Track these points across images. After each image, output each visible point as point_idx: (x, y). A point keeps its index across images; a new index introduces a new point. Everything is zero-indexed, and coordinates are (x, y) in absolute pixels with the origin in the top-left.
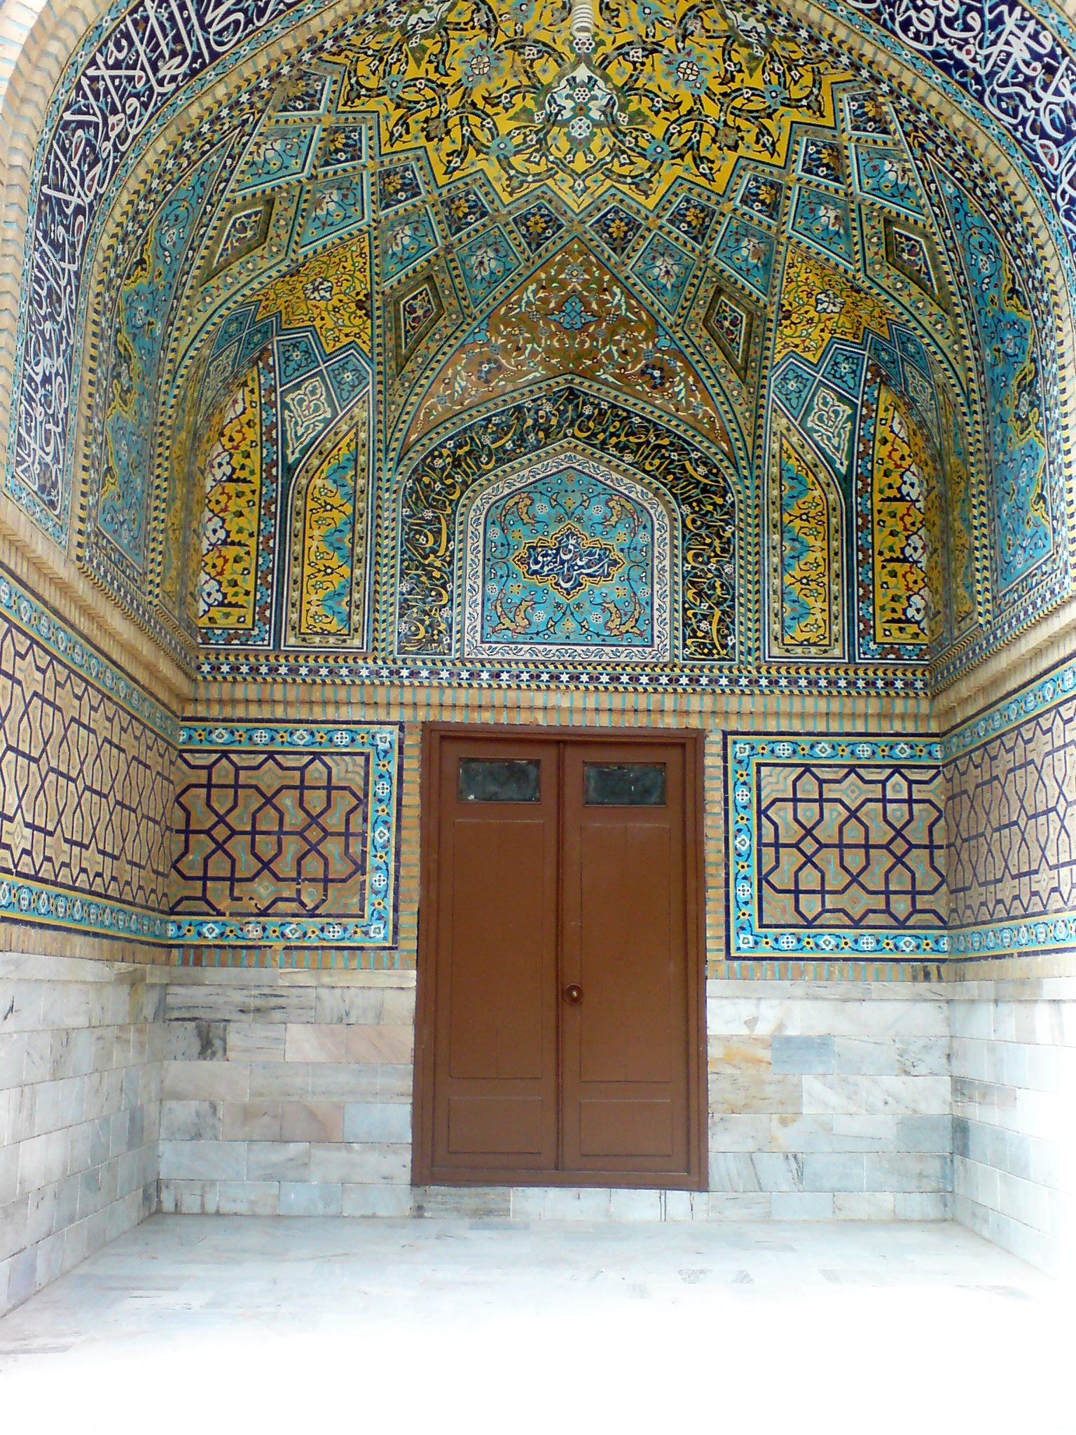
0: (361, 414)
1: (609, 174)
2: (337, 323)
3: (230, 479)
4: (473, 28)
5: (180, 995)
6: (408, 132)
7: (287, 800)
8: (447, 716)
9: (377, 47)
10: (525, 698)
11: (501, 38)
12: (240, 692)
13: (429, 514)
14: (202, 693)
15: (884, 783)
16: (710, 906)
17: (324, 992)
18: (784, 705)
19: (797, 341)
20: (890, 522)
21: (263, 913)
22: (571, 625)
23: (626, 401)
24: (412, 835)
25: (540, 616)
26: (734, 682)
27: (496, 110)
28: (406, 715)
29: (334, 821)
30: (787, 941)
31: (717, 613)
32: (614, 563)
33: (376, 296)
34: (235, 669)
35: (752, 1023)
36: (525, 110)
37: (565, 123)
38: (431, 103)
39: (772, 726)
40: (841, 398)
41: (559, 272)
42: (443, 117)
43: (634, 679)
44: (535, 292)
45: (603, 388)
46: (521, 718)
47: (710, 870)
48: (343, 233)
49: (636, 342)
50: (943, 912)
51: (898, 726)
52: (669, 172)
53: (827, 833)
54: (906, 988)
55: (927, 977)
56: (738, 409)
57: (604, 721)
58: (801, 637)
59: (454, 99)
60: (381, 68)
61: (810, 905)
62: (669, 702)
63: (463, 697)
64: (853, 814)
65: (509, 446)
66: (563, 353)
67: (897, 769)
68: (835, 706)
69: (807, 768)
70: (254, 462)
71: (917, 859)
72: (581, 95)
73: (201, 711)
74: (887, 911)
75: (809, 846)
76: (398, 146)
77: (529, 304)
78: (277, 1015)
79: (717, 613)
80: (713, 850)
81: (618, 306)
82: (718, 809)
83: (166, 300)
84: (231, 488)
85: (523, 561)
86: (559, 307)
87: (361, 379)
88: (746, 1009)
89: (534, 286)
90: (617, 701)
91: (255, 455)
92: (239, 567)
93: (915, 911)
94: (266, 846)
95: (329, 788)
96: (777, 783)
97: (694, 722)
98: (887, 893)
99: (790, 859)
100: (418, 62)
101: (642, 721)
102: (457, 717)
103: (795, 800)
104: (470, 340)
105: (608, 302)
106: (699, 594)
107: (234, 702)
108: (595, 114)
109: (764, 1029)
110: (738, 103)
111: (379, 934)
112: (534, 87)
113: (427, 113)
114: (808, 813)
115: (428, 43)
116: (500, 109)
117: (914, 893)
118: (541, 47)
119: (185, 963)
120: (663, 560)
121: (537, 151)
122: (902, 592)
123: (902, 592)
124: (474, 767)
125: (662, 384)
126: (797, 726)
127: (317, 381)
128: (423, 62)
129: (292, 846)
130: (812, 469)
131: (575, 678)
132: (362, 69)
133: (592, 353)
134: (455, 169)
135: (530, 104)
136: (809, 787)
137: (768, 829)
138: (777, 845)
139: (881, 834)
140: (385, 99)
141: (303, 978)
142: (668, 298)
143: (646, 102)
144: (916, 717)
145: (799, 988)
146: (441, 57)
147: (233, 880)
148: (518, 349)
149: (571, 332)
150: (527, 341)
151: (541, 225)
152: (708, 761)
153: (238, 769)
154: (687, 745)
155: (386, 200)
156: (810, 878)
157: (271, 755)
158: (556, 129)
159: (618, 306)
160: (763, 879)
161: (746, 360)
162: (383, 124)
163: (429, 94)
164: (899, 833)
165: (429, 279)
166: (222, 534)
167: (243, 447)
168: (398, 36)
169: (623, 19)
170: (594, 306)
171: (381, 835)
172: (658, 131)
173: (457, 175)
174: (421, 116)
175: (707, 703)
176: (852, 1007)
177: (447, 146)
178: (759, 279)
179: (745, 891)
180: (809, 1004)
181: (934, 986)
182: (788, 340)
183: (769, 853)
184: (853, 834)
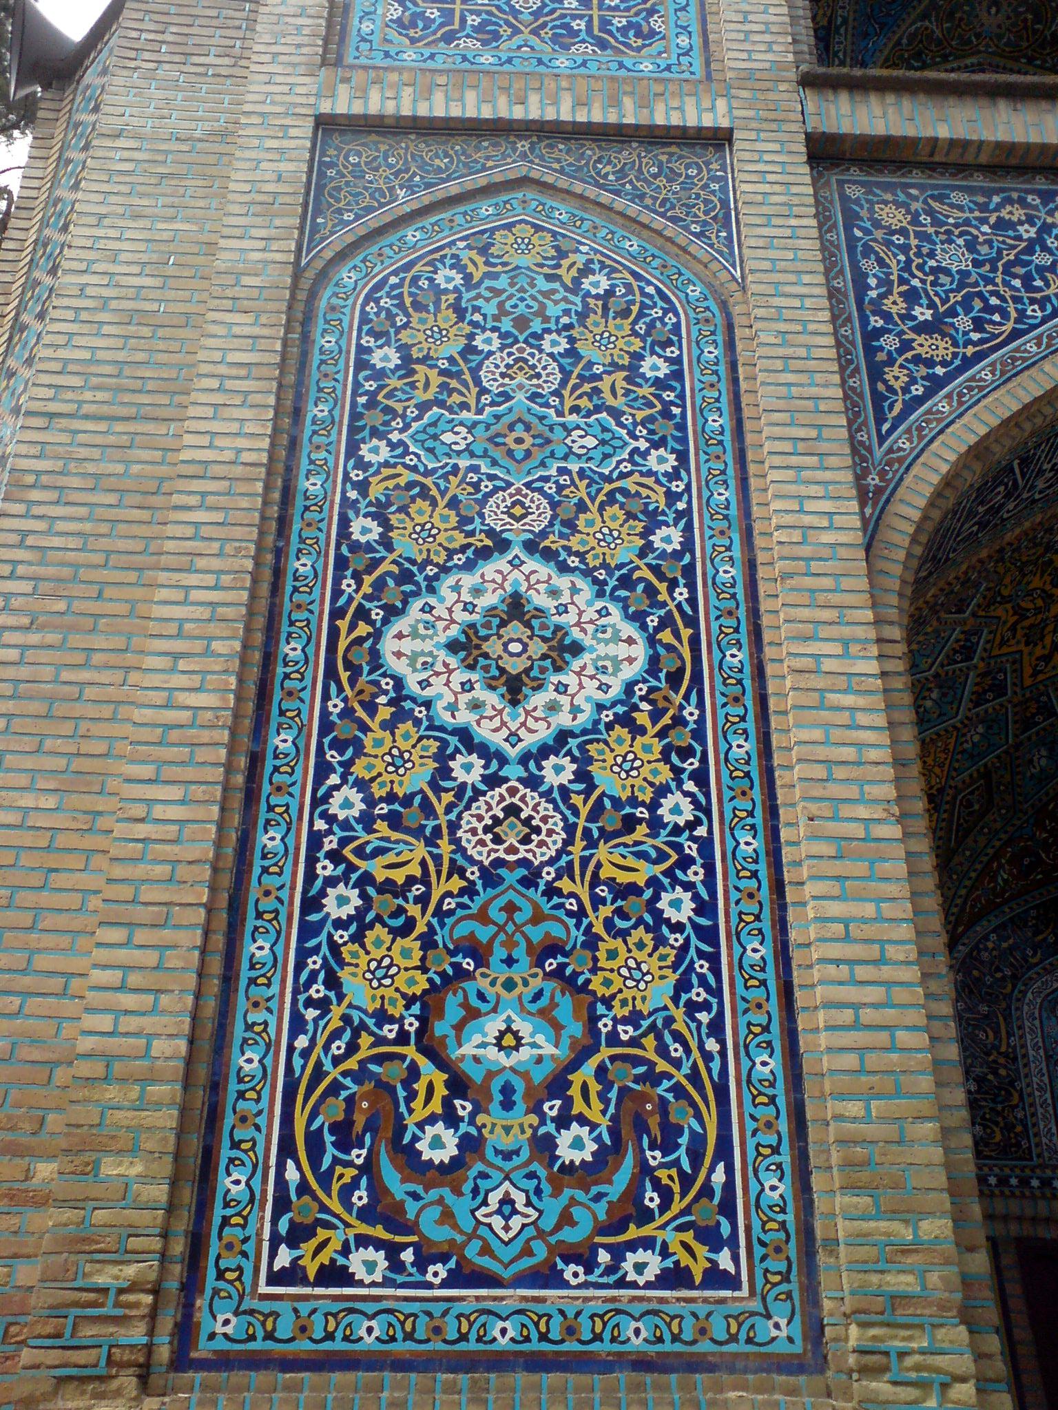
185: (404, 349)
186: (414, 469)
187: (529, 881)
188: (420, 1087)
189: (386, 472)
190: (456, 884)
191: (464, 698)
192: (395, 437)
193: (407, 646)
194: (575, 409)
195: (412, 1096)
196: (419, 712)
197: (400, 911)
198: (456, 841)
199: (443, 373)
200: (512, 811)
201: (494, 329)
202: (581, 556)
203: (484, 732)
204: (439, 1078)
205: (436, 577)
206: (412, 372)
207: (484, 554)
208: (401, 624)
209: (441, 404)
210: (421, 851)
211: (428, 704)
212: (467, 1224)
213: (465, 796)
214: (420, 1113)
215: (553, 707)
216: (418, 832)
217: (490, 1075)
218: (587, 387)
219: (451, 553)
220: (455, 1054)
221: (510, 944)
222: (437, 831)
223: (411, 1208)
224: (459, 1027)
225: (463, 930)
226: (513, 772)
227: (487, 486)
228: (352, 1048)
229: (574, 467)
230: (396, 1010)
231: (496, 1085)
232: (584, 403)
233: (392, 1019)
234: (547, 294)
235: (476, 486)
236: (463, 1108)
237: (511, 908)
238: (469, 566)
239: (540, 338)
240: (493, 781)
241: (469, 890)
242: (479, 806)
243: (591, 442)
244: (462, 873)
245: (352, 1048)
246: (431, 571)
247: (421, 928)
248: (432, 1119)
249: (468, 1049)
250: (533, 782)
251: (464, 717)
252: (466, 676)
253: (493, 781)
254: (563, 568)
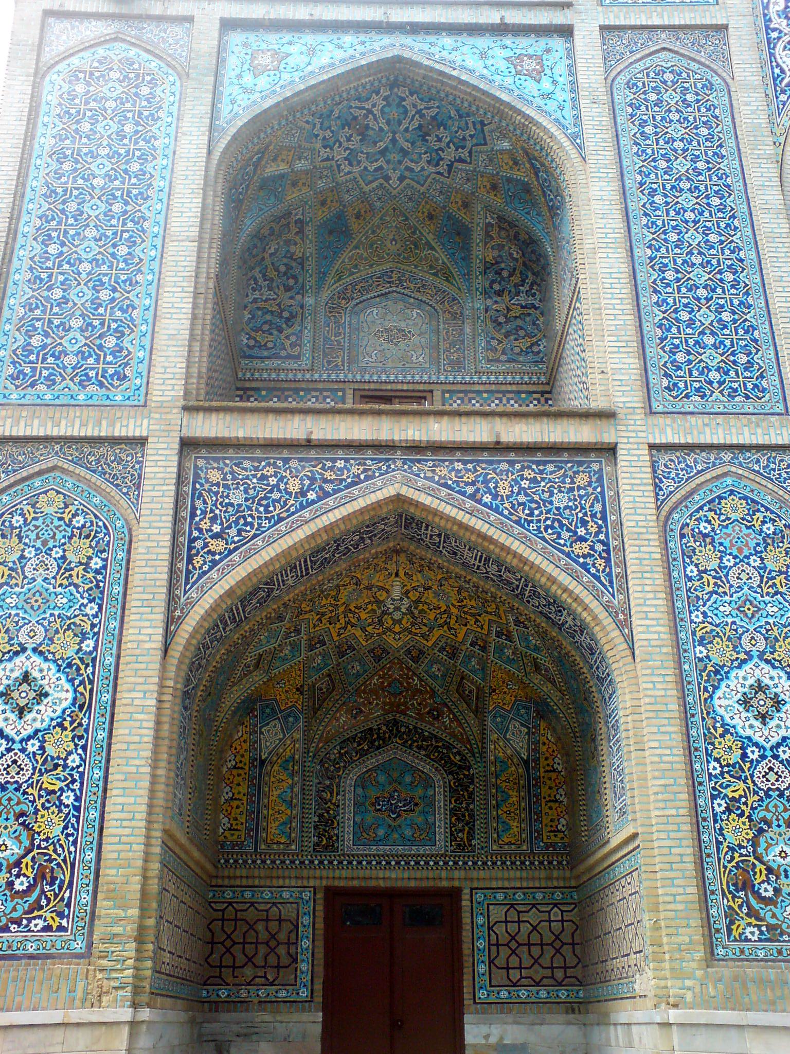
0: (296, 736)
2: (286, 696)
3: (235, 767)
5: (209, 1027)
7: (260, 927)
8: (336, 883)
10: (374, 873)
12: (238, 873)
13: (328, 782)
14: (221, 874)
15: (549, 912)
16: (465, 977)
17: (277, 1025)
18: (500, 874)
20: (548, 782)
21: (249, 984)
22: (396, 836)
23: (423, 726)
24: (320, 944)
25: (381, 832)
26: (475, 863)
28: (317, 883)
29: (282, 936)
30: (504, 994)
31: (467, 829)
32: (416, 805)
34: (236, 861)
35: (487, 1037)
38: (331, 612)
39: (494, 884)
40: (522, 725)
43: (427, 863)
45: (410, 720)
46: (373, 883)
47: (465, 958)
48: (292, 663)
49: (425, 700)
50: (580, 977)
51: (555, 884)
52: (437, 633)
53: (522, 938)
54: (562, 1018)
55: (573, 1011)
56: (474, 730)
57: (413, 884)
58: (507, 841)
61: (515, 975)
62: (444, 874)
63: (344, 873)
64: (535, 928)
65: (366, 748)
66: (390, 703)
67: (555, 905)
68: (524, 874)
69: (512, 905)
70: (246, 759)
71: (567, 950)
73: (220, 882)
74: (552, 977)
75: (513, 945)
78: (254, 1037)
79: (467, 829)
80: (466, 949)
82: (469, 927)
83: (216, 707)
84: (235, 772)
85: (373, 804)
86: (389, 685)
87: (296, 719)
88: (484, 1029)
90: (419, 874)
91: (247, 757)
92: (238, 811)
93: (566, 977)
94: (250, 950)
95: (280, 920)
96: (497, 913)
97: (456, 884)
98: (552, 968)
99: (504, 952)
101: (431, 883)
102: (342, 883)
103: (506, 922)
106: (458, 819)
107: (235, 877)
109: (493, 1040)
111: (304, 994)
114: (513, 928)
117: (565, 968)
119: (210, 1010)
120: (440, 801)
122: (555, 817)
123: (555, 817)
124: (349, 910)
126: (506, 884)
127: (277, 722)
129: (262, 950)
130: (510, 758)
131: (398, 863)
133: (405, 704)
135: (375, 607)
136: (513, 915)
137: (493, 937)
138: (498, 945)
139: (548, 938)
141: (267, 1017)
142: (439, 682)
144: (564, 879)
145: (510, 1018)
147: (234, 967)
149: (395, 695)
151: (379, 653)
152: (464, 903)
153: (237, 911)
154: (454, 894)
155: (311, 648)
156: (514, 961)
157: (252, 904)
160: (491, 962)
161: (477, 706)
164: (557, 937)
165: (329, 676)
166: (230, 795)
167: (242, 752)
171: (306, 943)
175: (462, 874)
176: (537, 1027)
177: (338, 626)
178: (480, 675)
179: (482, 968)
180: (515, 1026)
181: (576, 1016)
183: (494, 949)
184: (535, 938)
185: (696, 565)
186: (710, 623)
187: (781, 795)
188: (757, 870)
189: (702, 626)
190: (756, 798)
191: (747, 724)
192: (702, 609)
193: (724, 702)
194: (768, 594)
195: (755, 873)
196: (732, 730)
197: (739, 808)
198: (753, 782)
199: (714, 577)
200: (771, 769)
201: (730, 554)
202: (780, 661)
203: (756, 738)
204: (763, 867)
205: (728, 672)
206: (702, 578)
207: (744, 661)
208: (719, 693)
209: (716, 593)
210: (742, 785)
211: (734, 727)
212: (781, 918)
213: (754, 764)
214: (759, 881)
215: (778, 726)
216: (739, 778)
217: (779, 866)
218: (770, 583)
219: (732, 661)
220: (766, 859)
221: (778, 820)
222: (746, 778)
223: (762, 912)
224: (766, 849)
225: (762, 814)
226: (769, 753)
227: (740, 631)
228: (733, 858)
229: (771, 621)
230: (745, 844)
231: (782, 869)
232: (770, 590)
233: (744, 847)
234: (748, 535)
235: (736, 630)
236: (773, 878)
237: (776, 806)
238: (739, 667)
239: (747, 557)
240: (763, 757)
241: (761, 800)
242: (759, 768)
243: (775, 609)
244: (757, 793)
245: (733, 858)
246: (726, 669)
247: (747, 814)
248: (763, 882)
249: (770, 857)
250: (775, 757)
251: (749, 732)
252: (747, 714)
253: (763, 757)
254: (774, 667)
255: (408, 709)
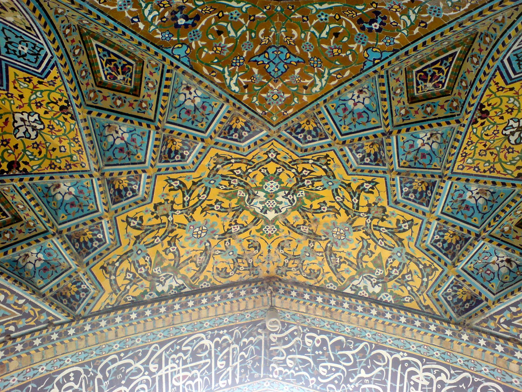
1: (249, 163)
4: (341, 257)
6: (398, 221)
9: (403, 288)
11: (324, 244)
19: (41, 87)
27: (333, 204)
33: (466, 123)
36: (312, 199)
37: (283, 189)
38: (377, 227)
41: (291, 99)
42: (371, 216)
44: (313, 84)
59: (360, 222)
60: (405, 272)
72: (272, 203)
76: (409, 217)
77: (321, 75)
81: (232, 74)
86: (290, 68)
89: (315, 90)
100: (379, 257)
104: (385, 55)
105: (243, 77)
108: (261, 194)
110: (162, 231)
112: (304, 211)
113: (381, 224)
115: (371, 265)
116: (329, 204)
118: (298, 231)
121: (304, 176)
125: (173, 13)
128: (376, 255)
132: (417, 282)
134: (369, 182)
140: (407, 250)
143: (226, 205)
146: (364, 251)
148: (336, 35)
150: (326, 41)
158: (290, 185)
159: (232, 74)
162: (415, 236)
163: (376, 233)
168: (390, 284)
169: (245, 244)
170: (256, 71)
172: (214, 194)
173: (369, 179)
174: (385, 224)
177: (372, 198)
182: (52, 88)
255: (246, 16)
